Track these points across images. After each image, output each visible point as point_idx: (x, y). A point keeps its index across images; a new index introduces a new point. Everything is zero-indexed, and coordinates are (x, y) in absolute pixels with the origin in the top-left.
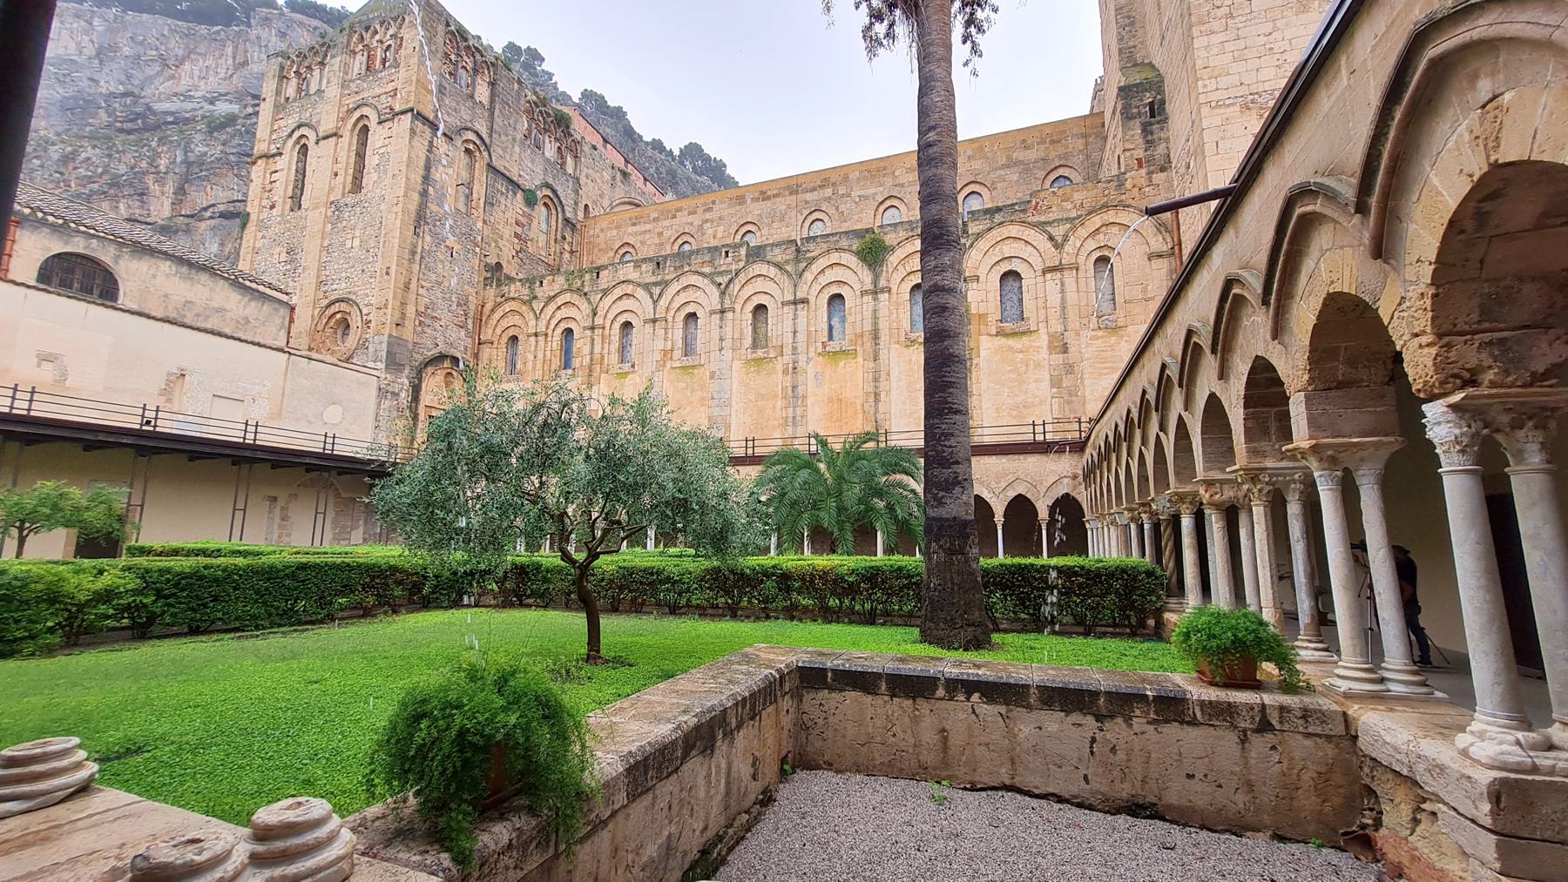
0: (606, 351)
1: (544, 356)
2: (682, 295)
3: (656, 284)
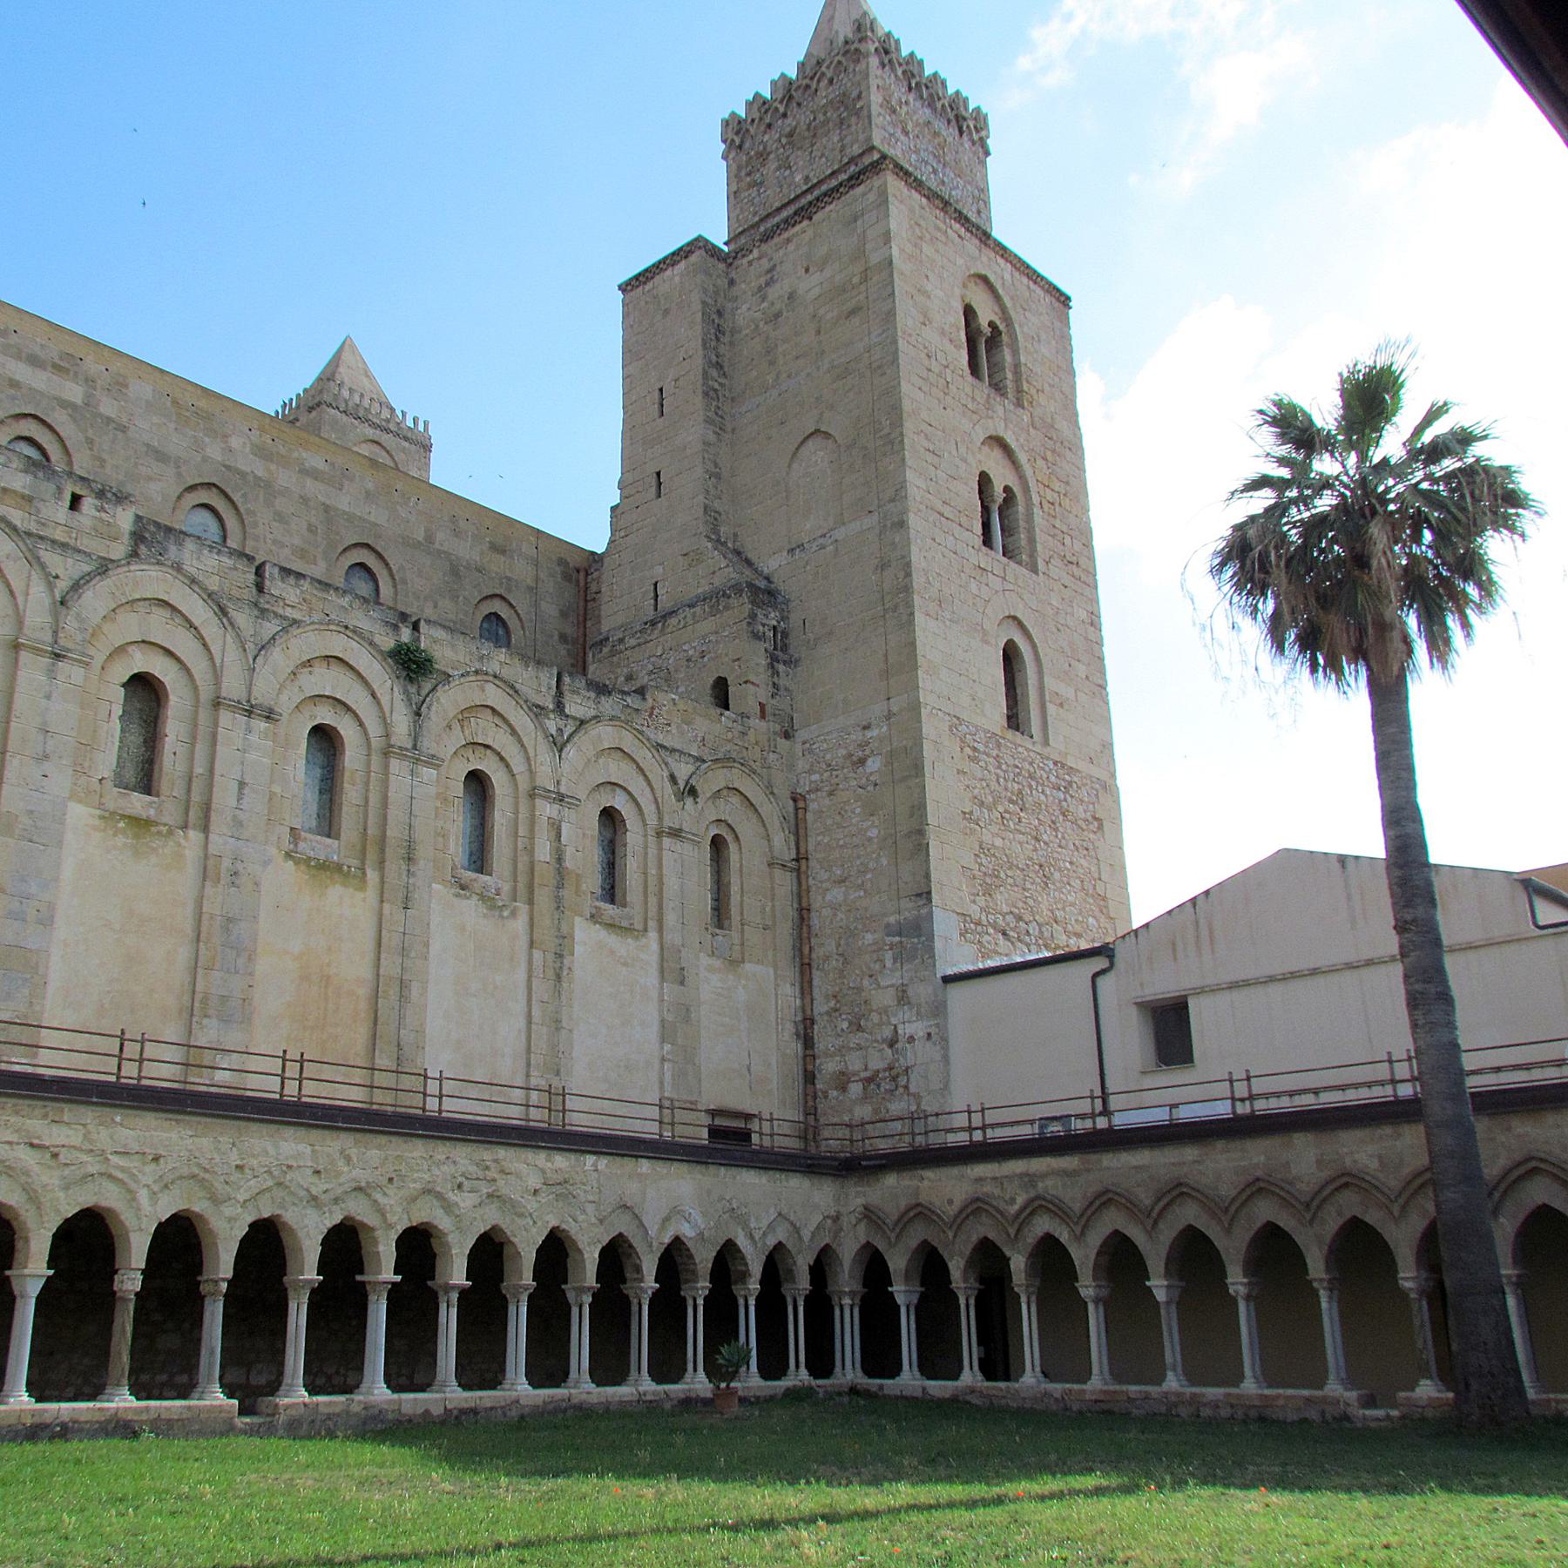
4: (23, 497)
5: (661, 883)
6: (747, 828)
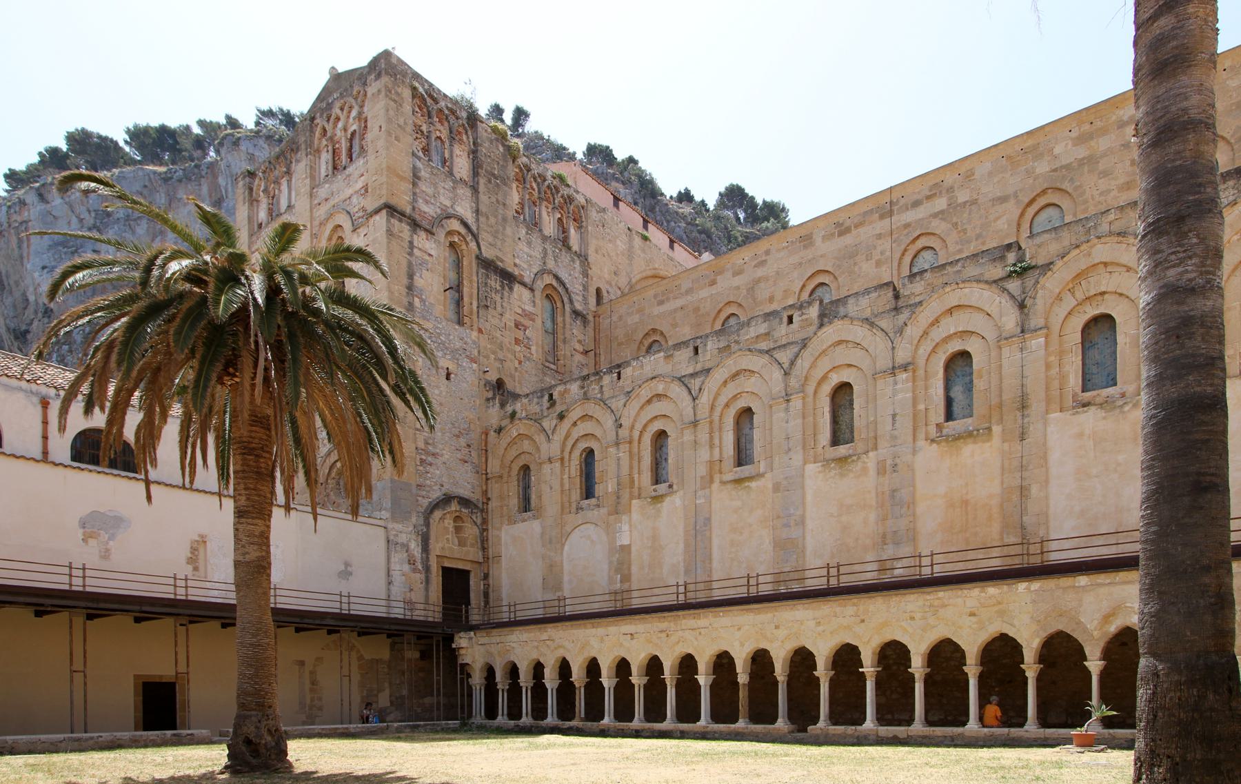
0: (636, 471)
1: (562, 485)
2: (731, 385)
3: (693, 375)
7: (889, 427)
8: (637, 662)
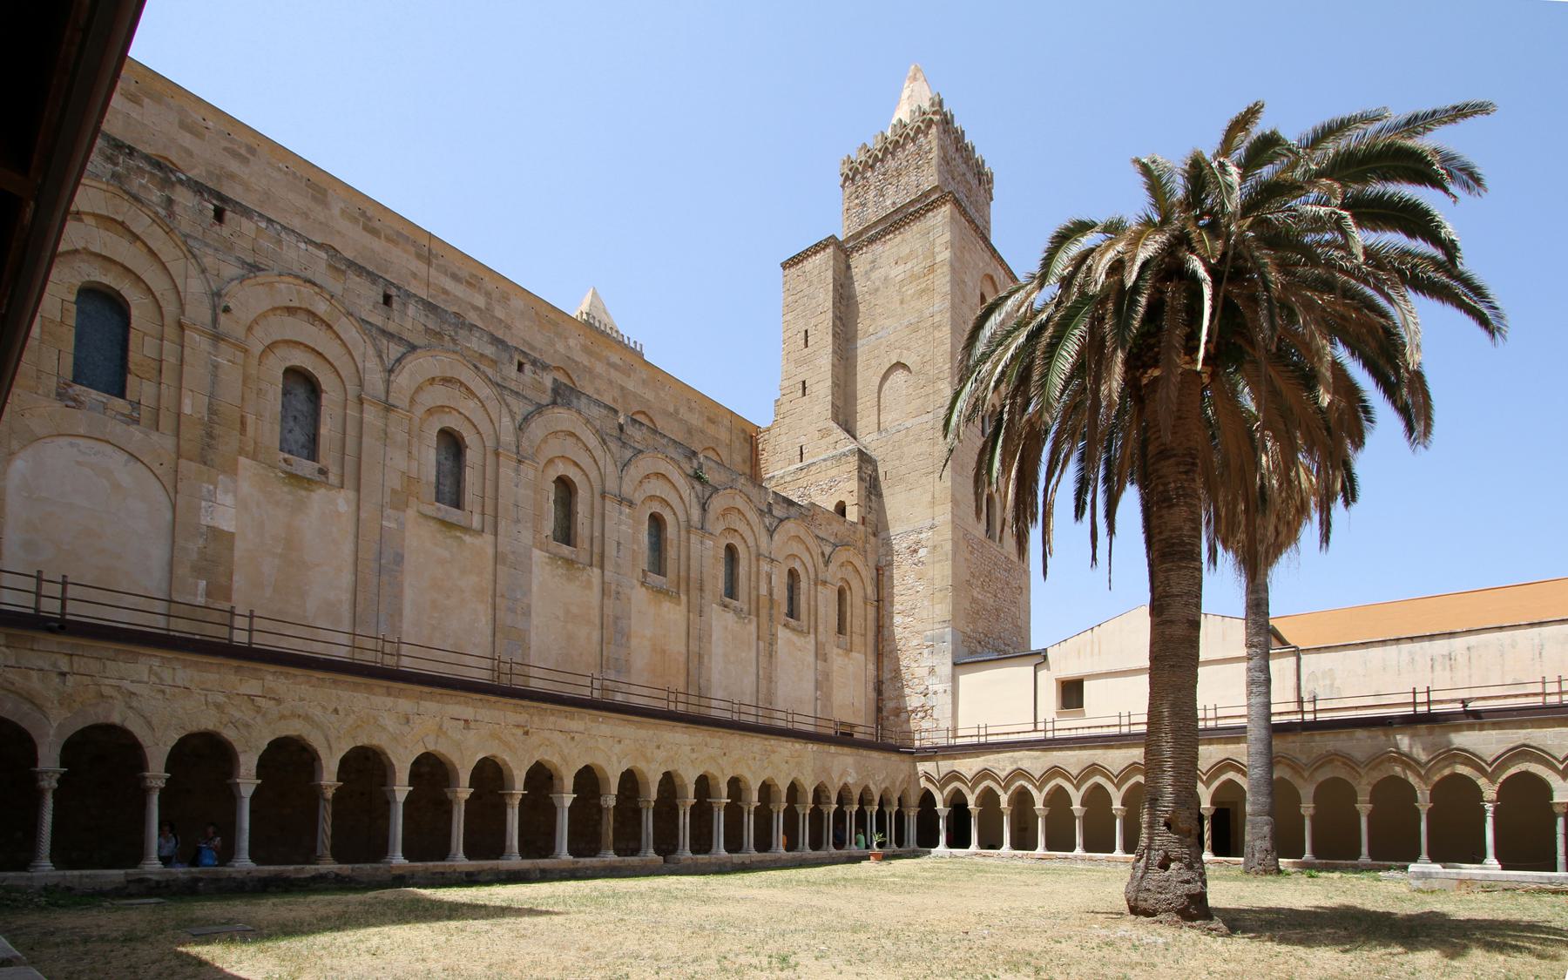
4: (492, 360)
5: (816, 610)
6: (855, 584)
7: (615, 553)
8: (689, 778)
